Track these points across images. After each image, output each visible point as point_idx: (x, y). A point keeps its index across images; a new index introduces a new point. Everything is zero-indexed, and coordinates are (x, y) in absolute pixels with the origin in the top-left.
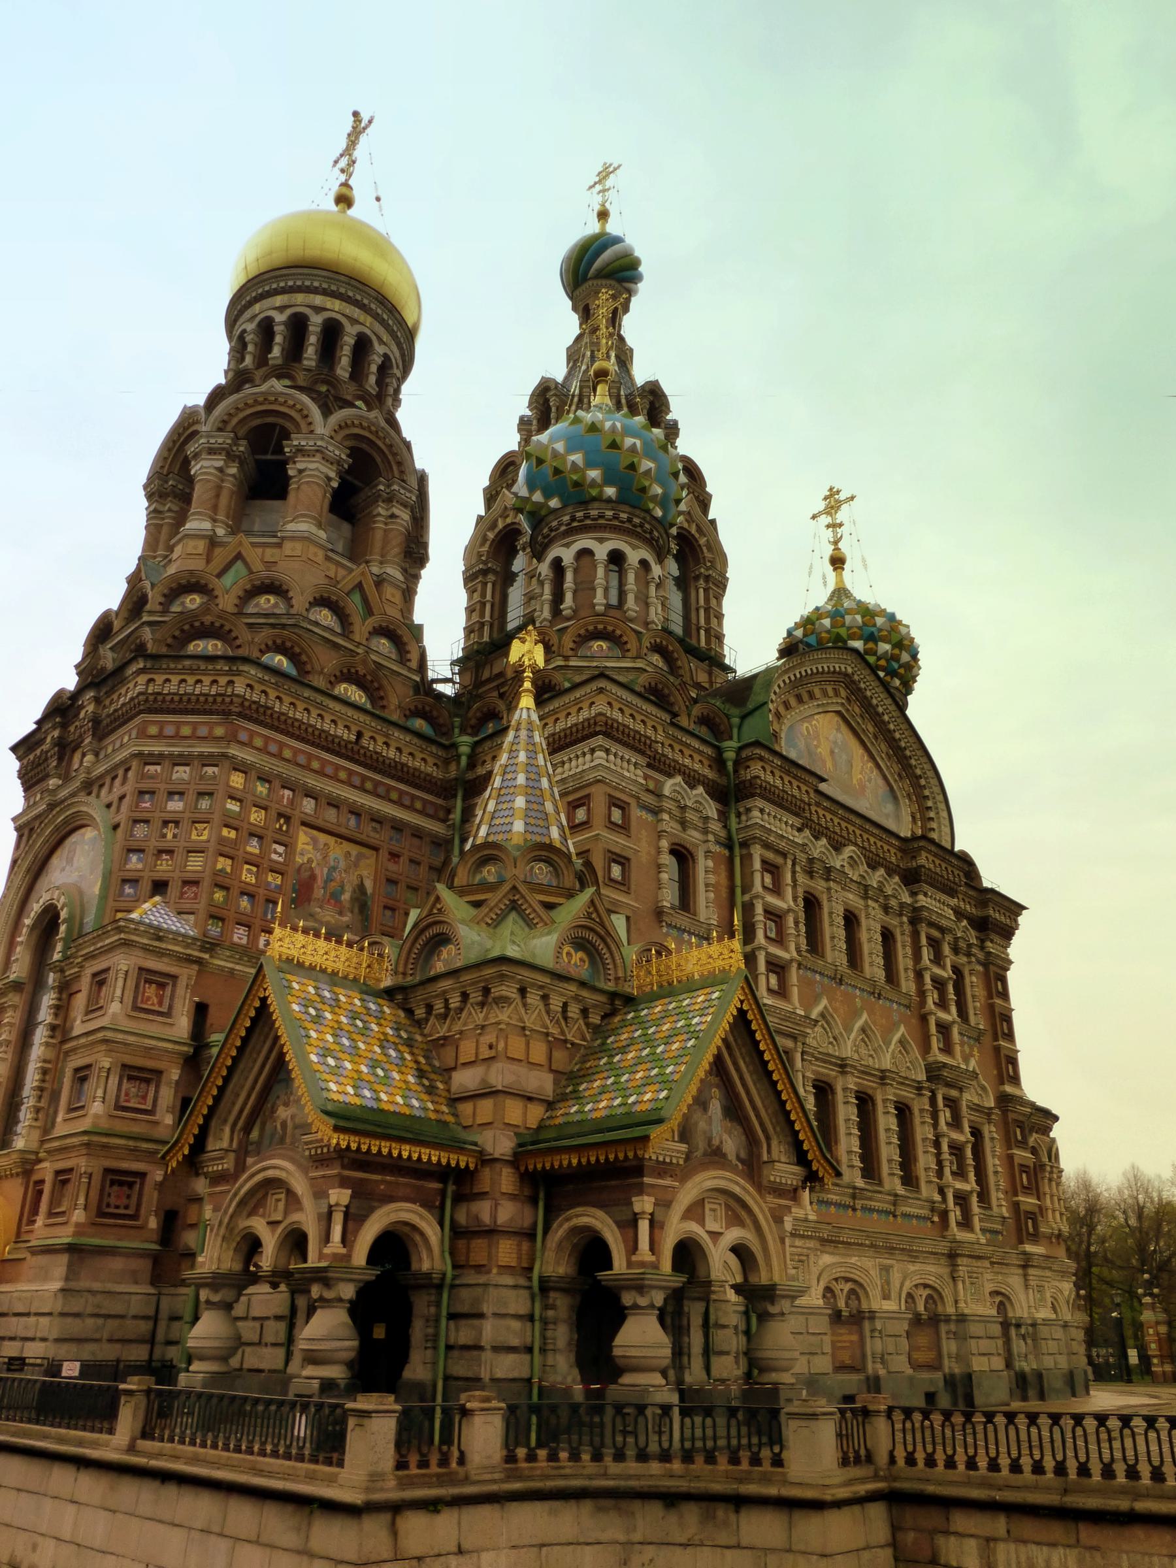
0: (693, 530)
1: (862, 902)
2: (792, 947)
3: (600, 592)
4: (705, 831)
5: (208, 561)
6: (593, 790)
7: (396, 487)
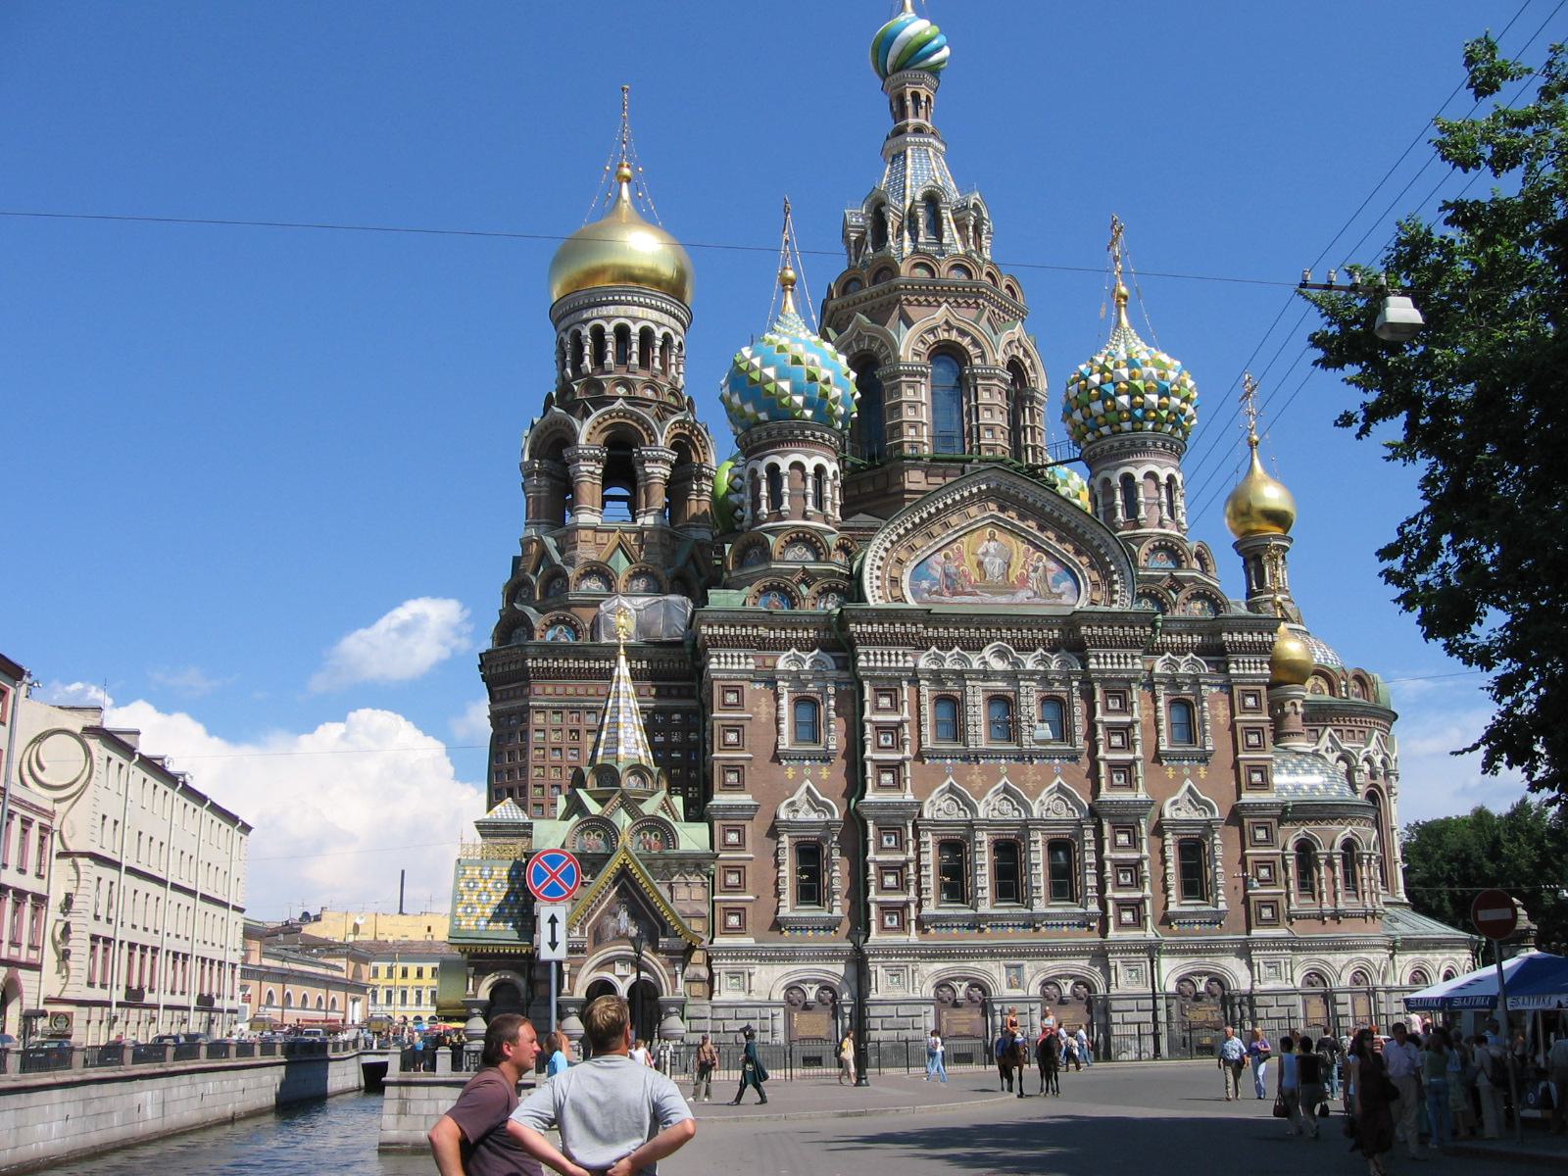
0: (954, 336)
3: (764, 503)
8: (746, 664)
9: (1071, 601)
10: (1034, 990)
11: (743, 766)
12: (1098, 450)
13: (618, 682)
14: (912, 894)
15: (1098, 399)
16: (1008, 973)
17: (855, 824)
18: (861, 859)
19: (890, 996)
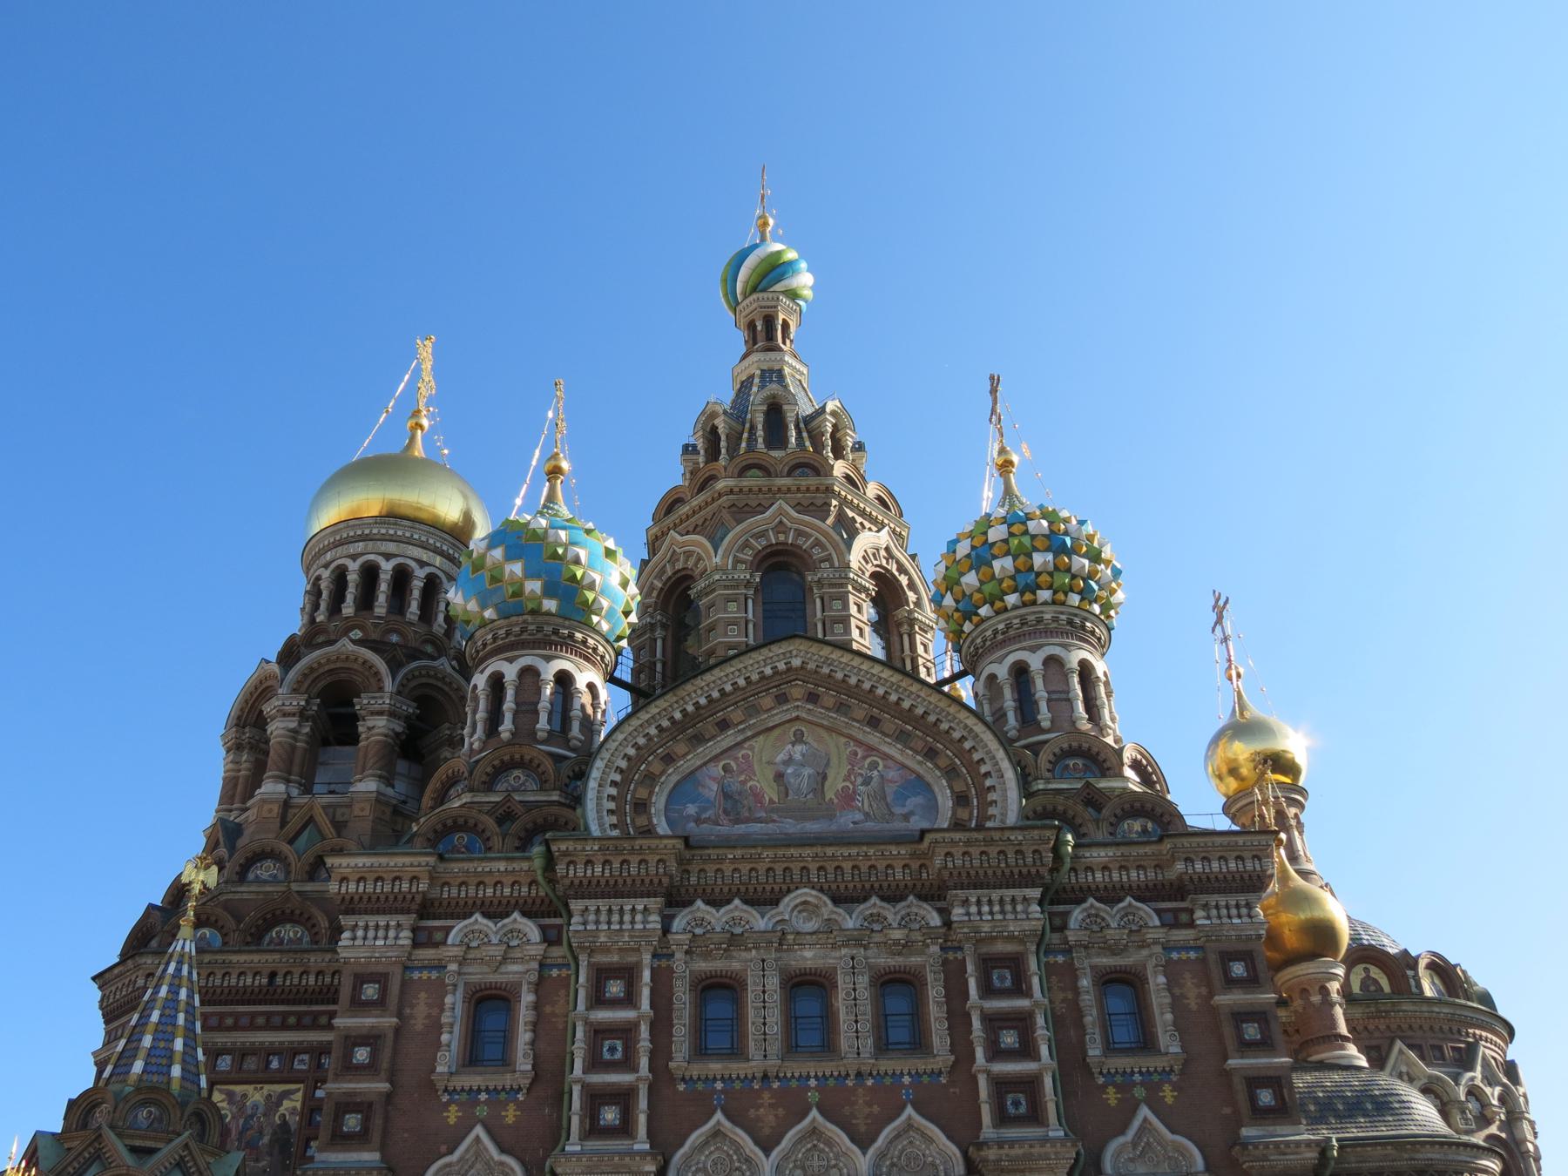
1: (837, 954)
4: (521, 960)
7: (365, 702)
8: (396, 938)
9: (925, 825)
11: (370, 1105)
12: (979, 640)
13: (168, 964)
15: (970, 570)
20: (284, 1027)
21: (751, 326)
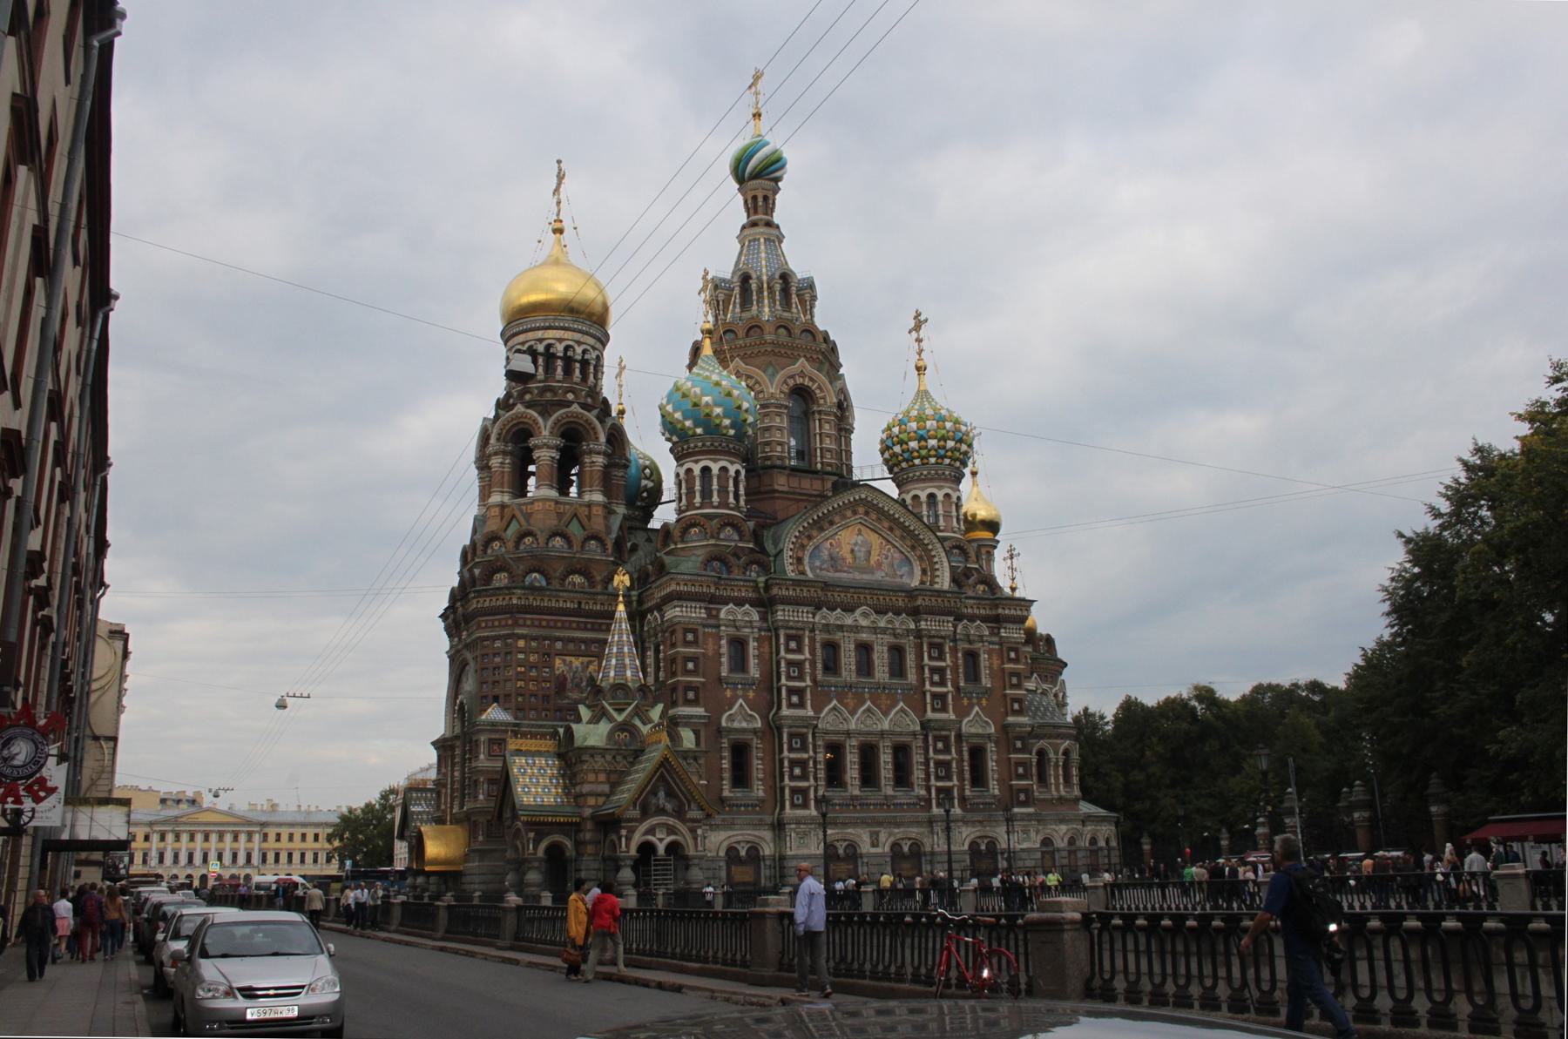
2: (808, 678)
3: (698, 495)
4: (752, 627)
5: (502, 519)
6: (676, 627)
9: (908, 581)
10: (887, 849)
11: (698, 688)
13: (620, 622)
14: (812, 781)
16: (871, 837)
17: (773, 729)
18: (777, 757)
19: (800, 852)
20: (585, 629)
21: (755, 198)
